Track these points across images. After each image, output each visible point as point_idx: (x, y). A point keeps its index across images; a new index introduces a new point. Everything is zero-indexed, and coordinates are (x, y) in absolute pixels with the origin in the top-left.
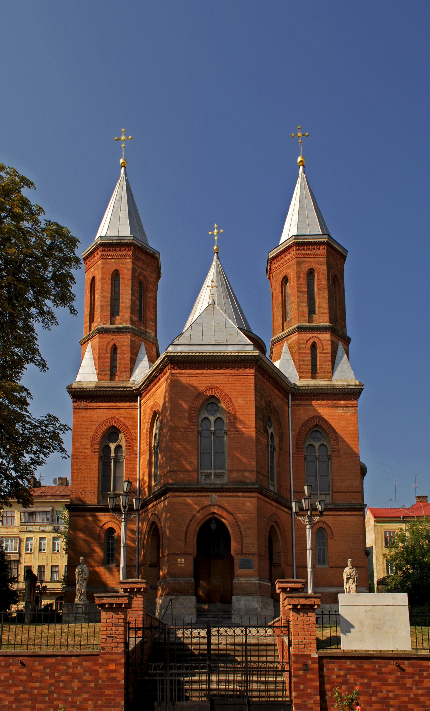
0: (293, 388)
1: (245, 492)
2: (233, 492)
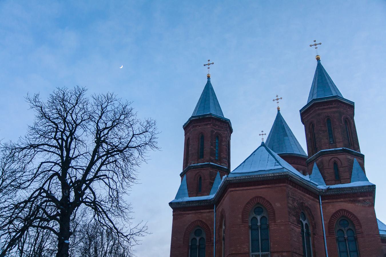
0: (321, 192)
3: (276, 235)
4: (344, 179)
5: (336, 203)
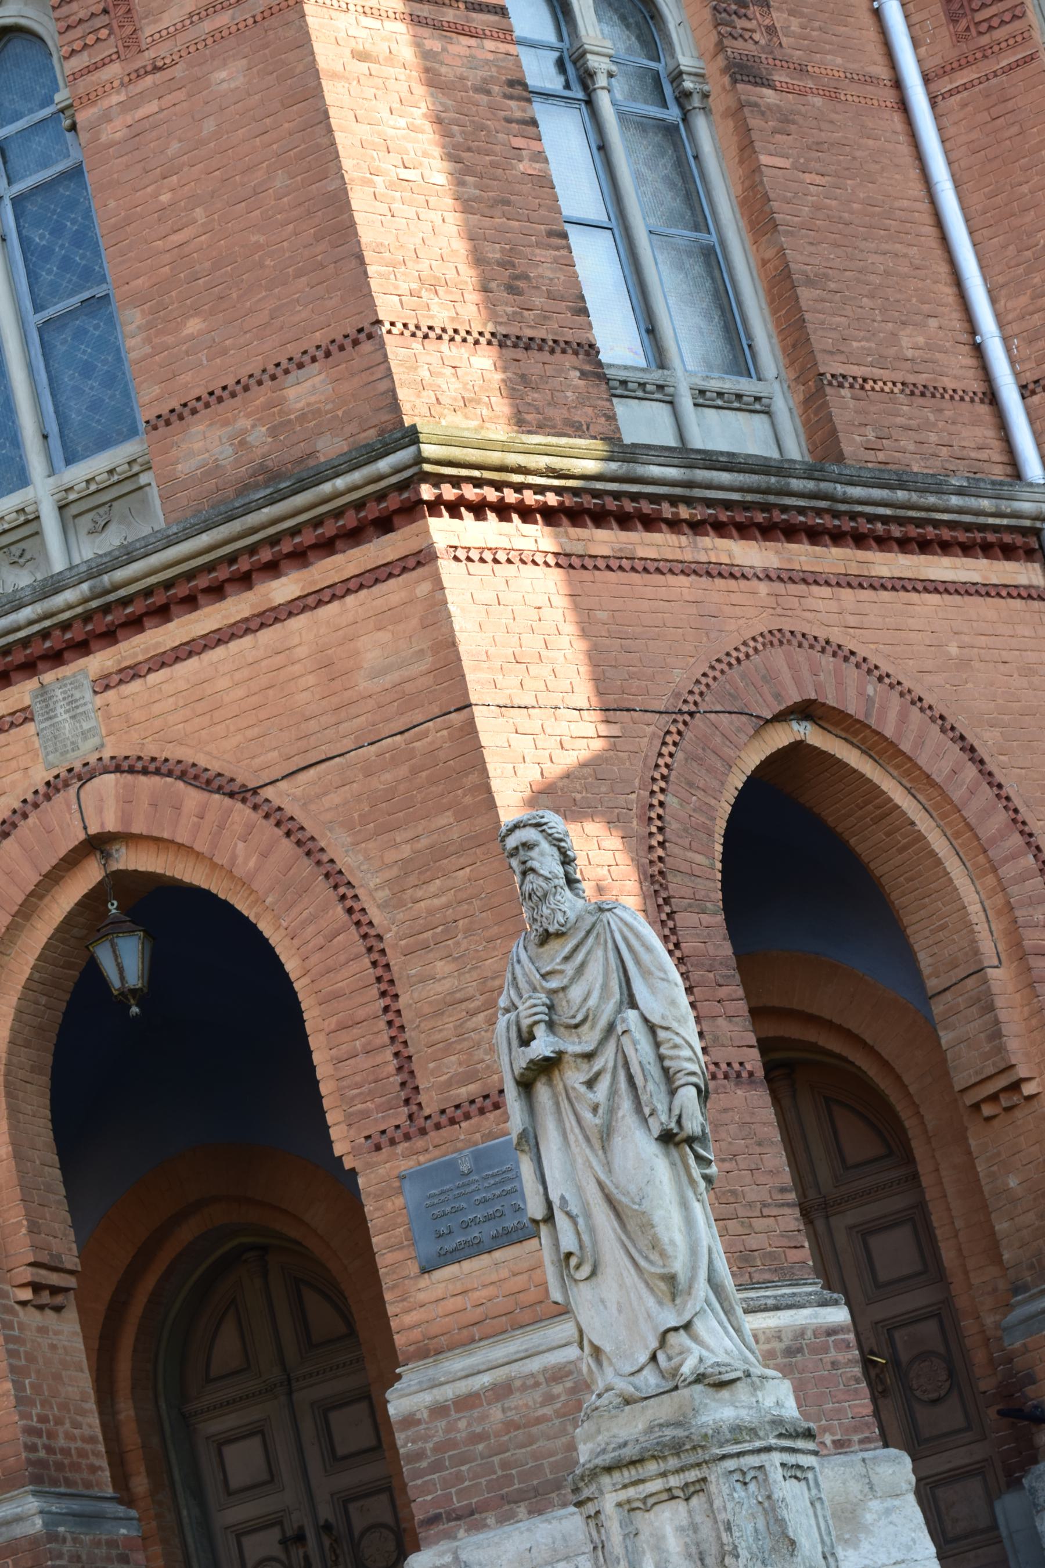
1: (328, 547)
2: (217, 592)
3: (165, 198)
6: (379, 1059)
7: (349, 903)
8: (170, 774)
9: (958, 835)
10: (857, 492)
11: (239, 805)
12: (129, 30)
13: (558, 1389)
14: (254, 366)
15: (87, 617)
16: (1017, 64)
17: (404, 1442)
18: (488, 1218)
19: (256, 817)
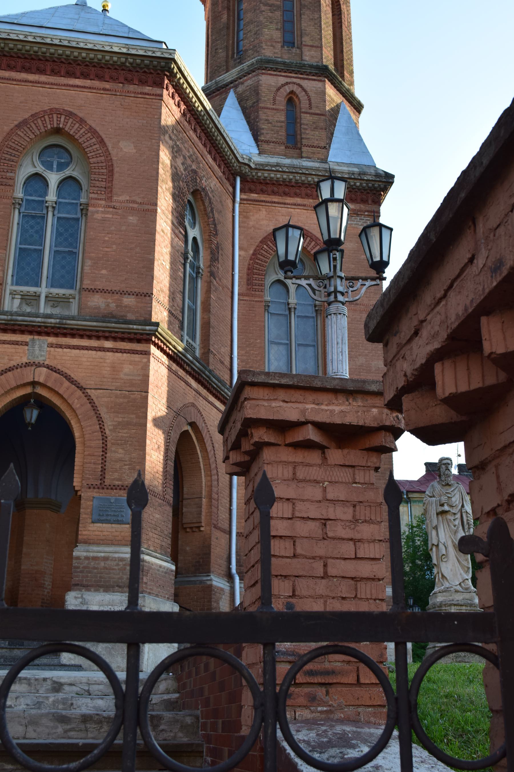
0: (245, 164)
1: (123, 339)
2: (90, 337)
3: (106, 239)
4: (313, 146)
5: (282, 206)
6: (97, 466)
7: (101, 426)
8: (62, 375)
9: (206, 465)
10: (214, 379)
11: (79, 391)
12: (110, 195)
13: (121, 563)
14: (117, 289)
15: (53, 328)
16: (259, 301)
17: (75, 563)
18: (114, 516)
19: (83, 395)
